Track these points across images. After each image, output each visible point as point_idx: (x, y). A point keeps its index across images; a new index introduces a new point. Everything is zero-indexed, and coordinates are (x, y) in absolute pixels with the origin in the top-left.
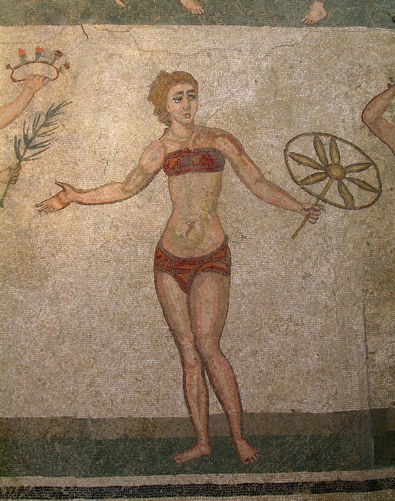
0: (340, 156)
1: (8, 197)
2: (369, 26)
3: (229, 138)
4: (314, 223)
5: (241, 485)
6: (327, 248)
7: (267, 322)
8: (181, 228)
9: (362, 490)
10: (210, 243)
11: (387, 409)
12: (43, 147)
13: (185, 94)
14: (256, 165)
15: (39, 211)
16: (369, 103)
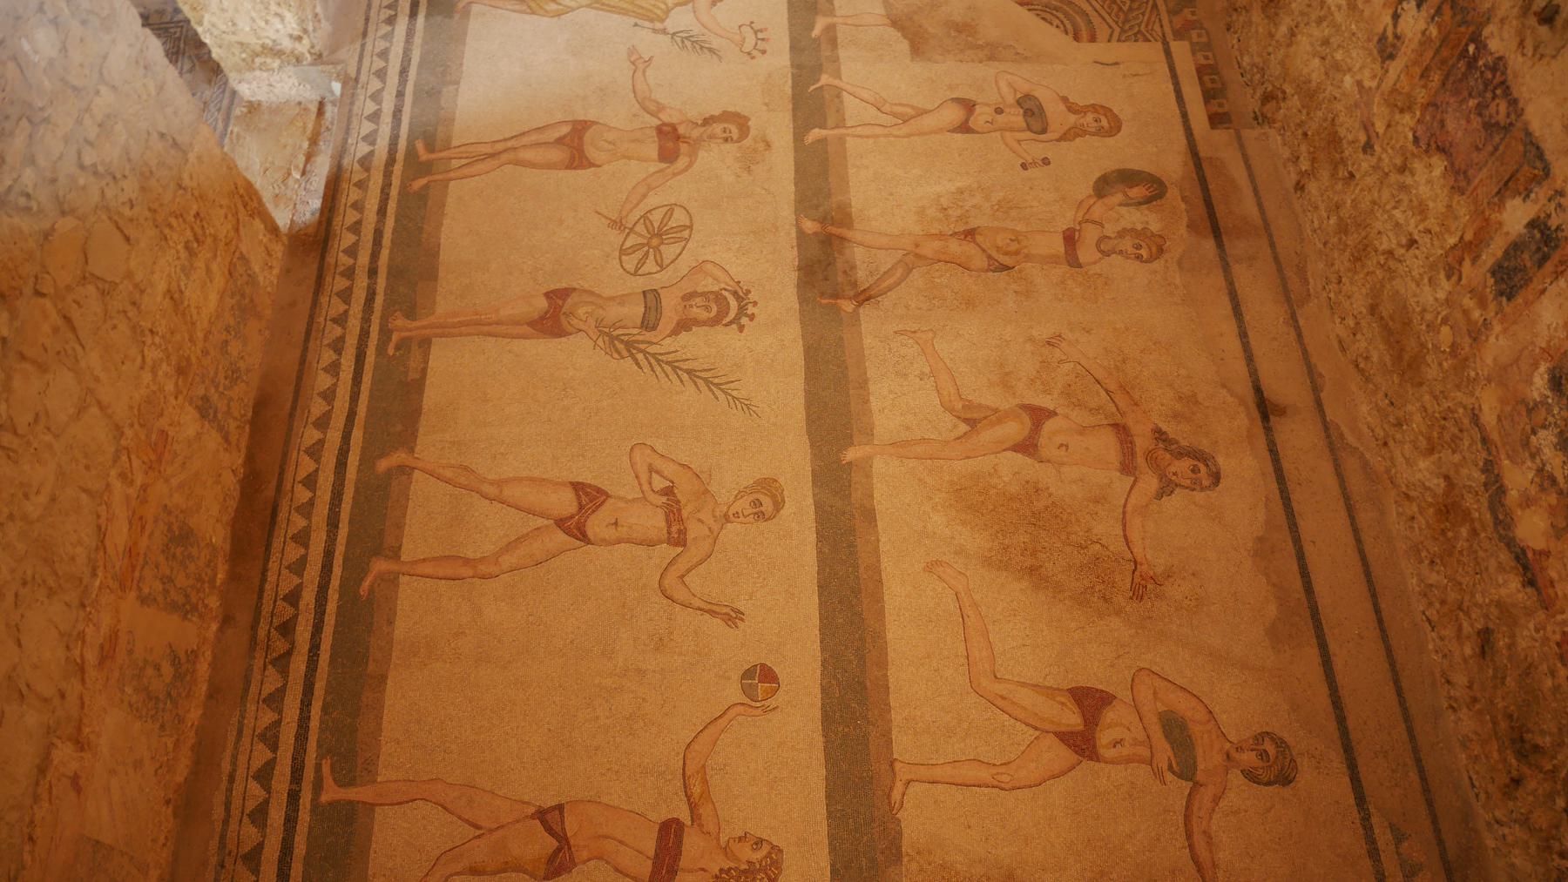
8: (610, 136)
9: (371, 263)
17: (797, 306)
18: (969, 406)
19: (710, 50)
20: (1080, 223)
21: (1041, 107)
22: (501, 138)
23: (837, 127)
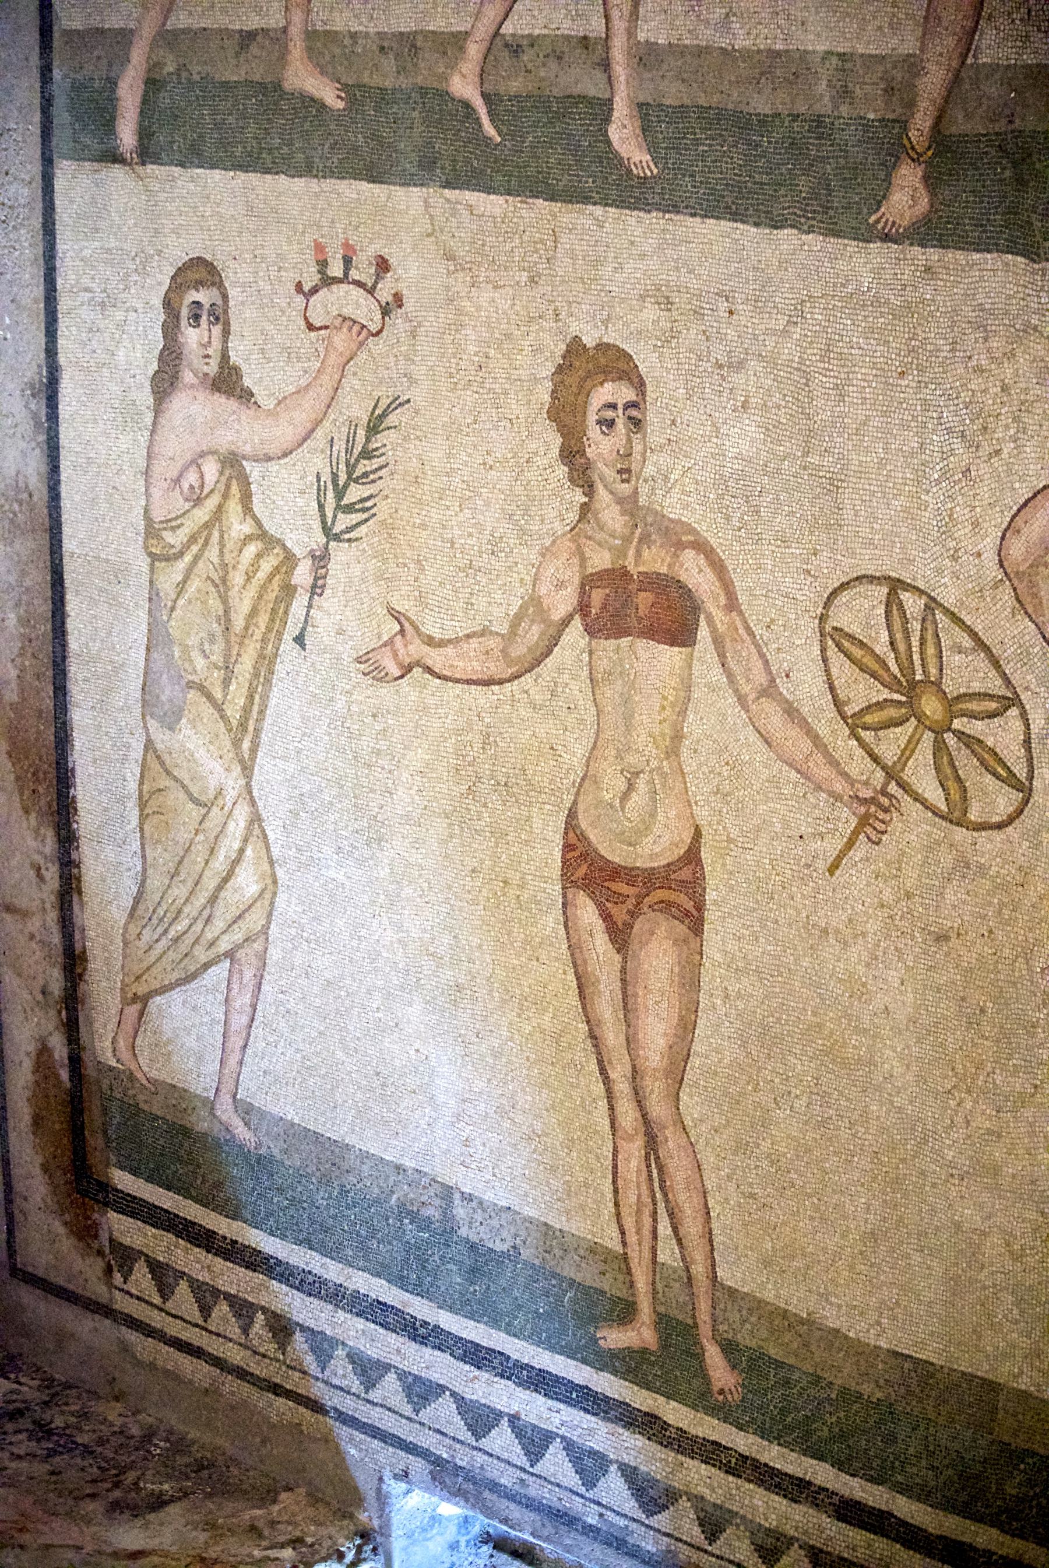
0: (941, 662)
1: (313, 626)
3: (707, 557)
4: (877, 844)
5: (708, 1441)
6: (901, 920)
7: (769, 1078)
8: (613, 783)
10: (665, 841)
11: (1000, 1384)
12: (364, 510)
13: (620, 411)
14: (759, 645)
15: (364, 674)
16: (1019, 510)
19: (374, 428)
22: (603, 1104)
23: (606, 65)
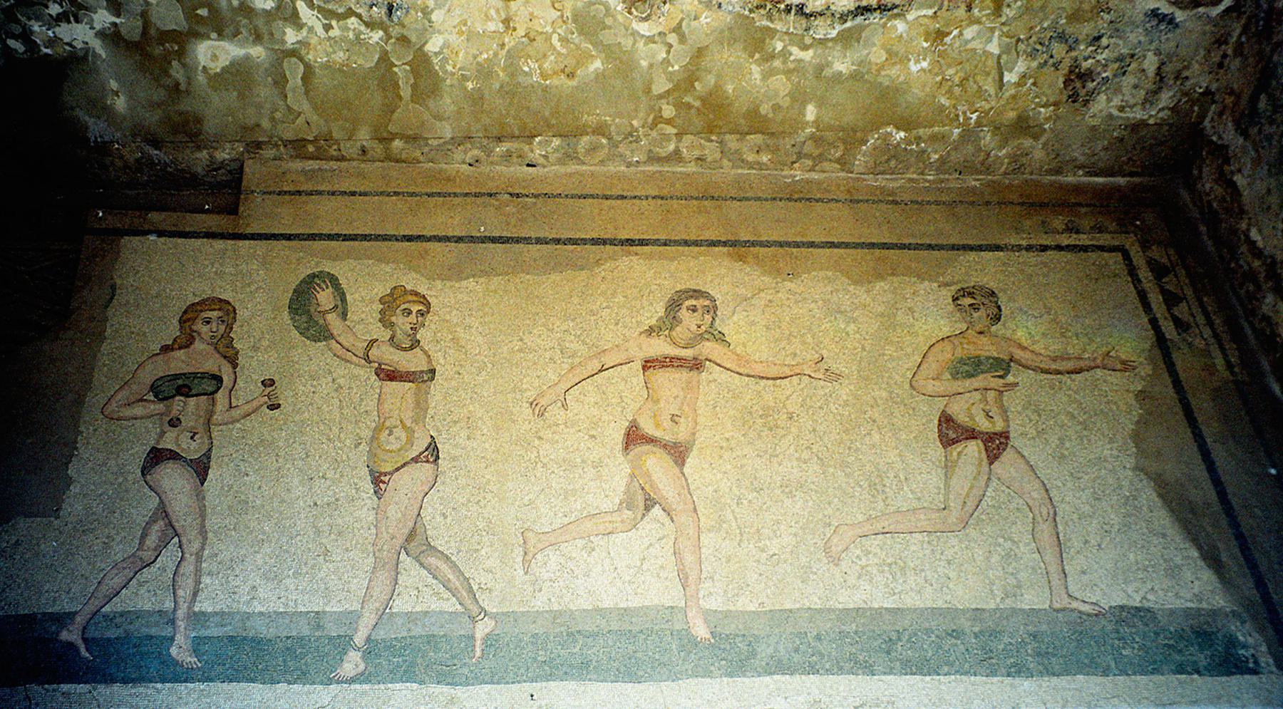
2: (422, 682)
17: (487, 687)
18: (628, 503)
20: (370, 362)
21: (176, 377)
23: (172, 622)
